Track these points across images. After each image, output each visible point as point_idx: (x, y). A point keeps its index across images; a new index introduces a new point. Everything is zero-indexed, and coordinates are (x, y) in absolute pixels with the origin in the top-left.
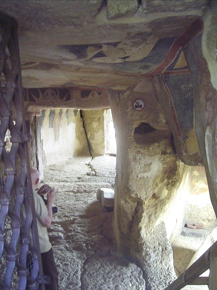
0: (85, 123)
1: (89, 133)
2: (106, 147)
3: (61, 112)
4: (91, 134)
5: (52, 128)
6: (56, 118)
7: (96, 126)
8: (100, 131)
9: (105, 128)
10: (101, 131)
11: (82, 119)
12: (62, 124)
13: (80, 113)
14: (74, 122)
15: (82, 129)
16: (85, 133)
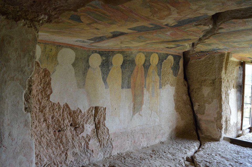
0: (190, 88)
1: (196, 103)
2: (224, 126)
3: (147, 64)
4: (199, 105)
5: (130, 90)
6: (137, 72)
7: (208, 93)
8: (214, 100)
9: (223, 97)
10: (215, 101)
11: (186, 83)
12: (149, 84)
13: (183, 73)
14: (172, 85)
15: (185, 97)
16: (190, 104)
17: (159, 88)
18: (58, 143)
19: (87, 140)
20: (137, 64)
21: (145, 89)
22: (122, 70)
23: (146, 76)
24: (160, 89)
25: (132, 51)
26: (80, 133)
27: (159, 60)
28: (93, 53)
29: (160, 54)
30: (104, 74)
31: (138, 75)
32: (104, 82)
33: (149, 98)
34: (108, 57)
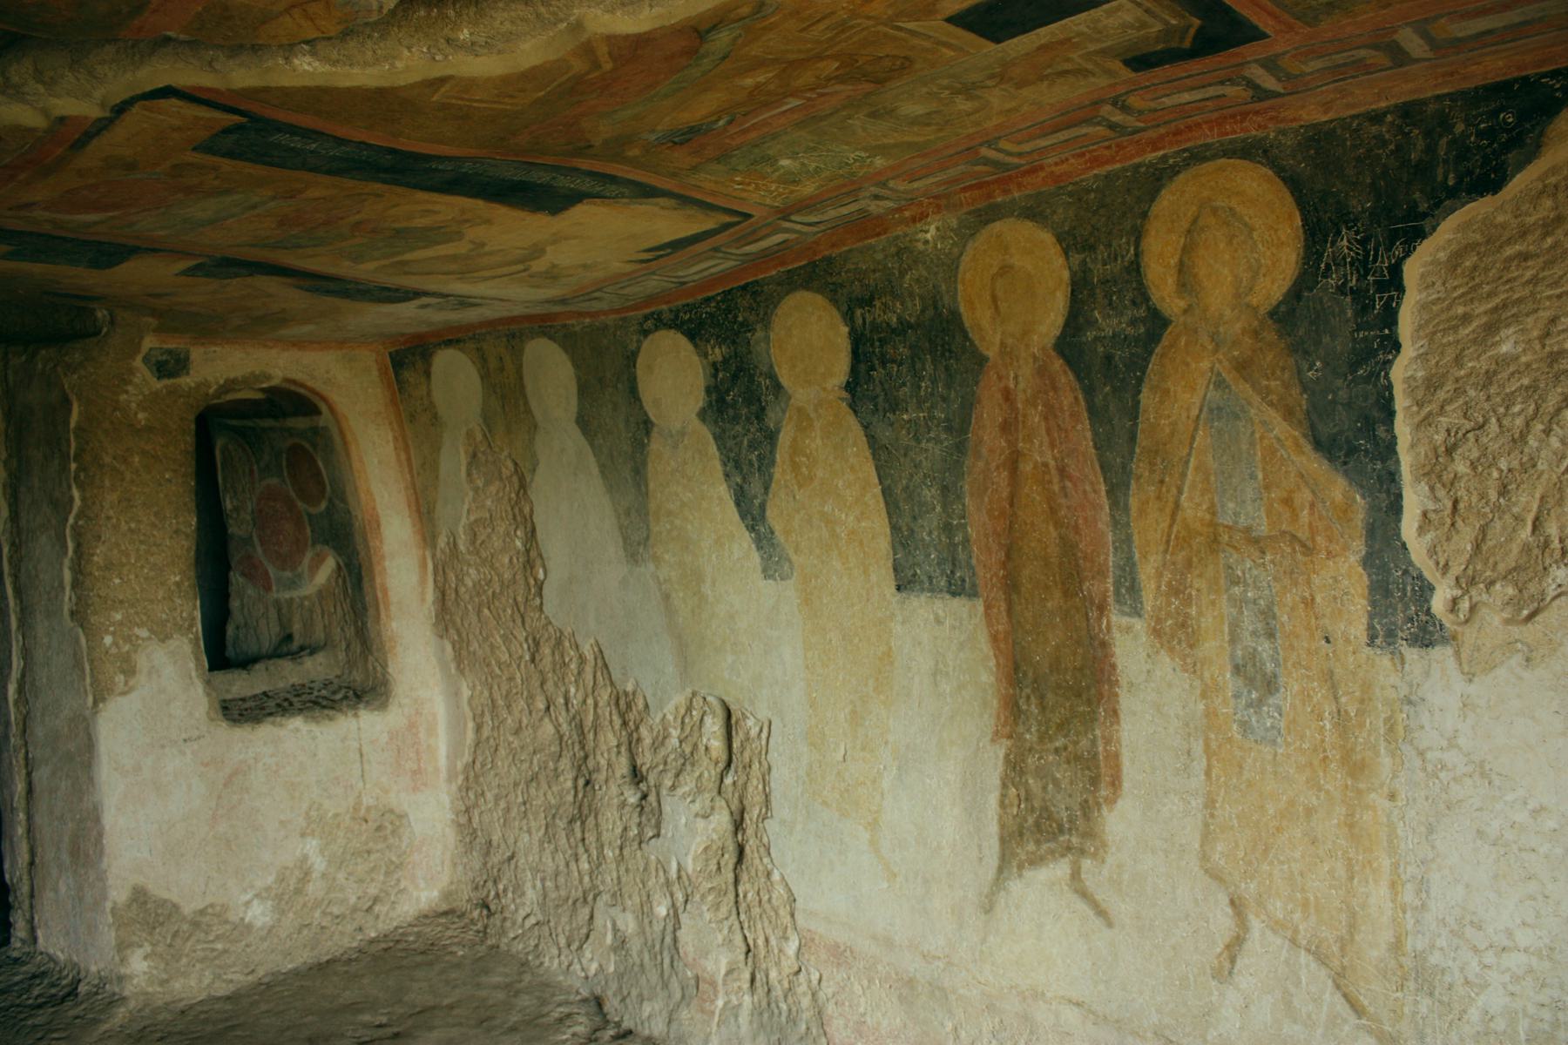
3: (1108, 323)
17: (1382, 635)
18: (572, 840)
19: (680, 897)
20: (991, 353)
21: (1139, 625)
22: (866, 427)
23: (1125, 470)
24: (1412, 654)
25: (899, 231)
26: (651, 838)
27: (1316, 234)
28: (646, 333)
29: (1319, 140)
30: (738, 466)
31: (1026, 467)
32: (752, 528)
33: (1198, 748)
34: (737, 334)
